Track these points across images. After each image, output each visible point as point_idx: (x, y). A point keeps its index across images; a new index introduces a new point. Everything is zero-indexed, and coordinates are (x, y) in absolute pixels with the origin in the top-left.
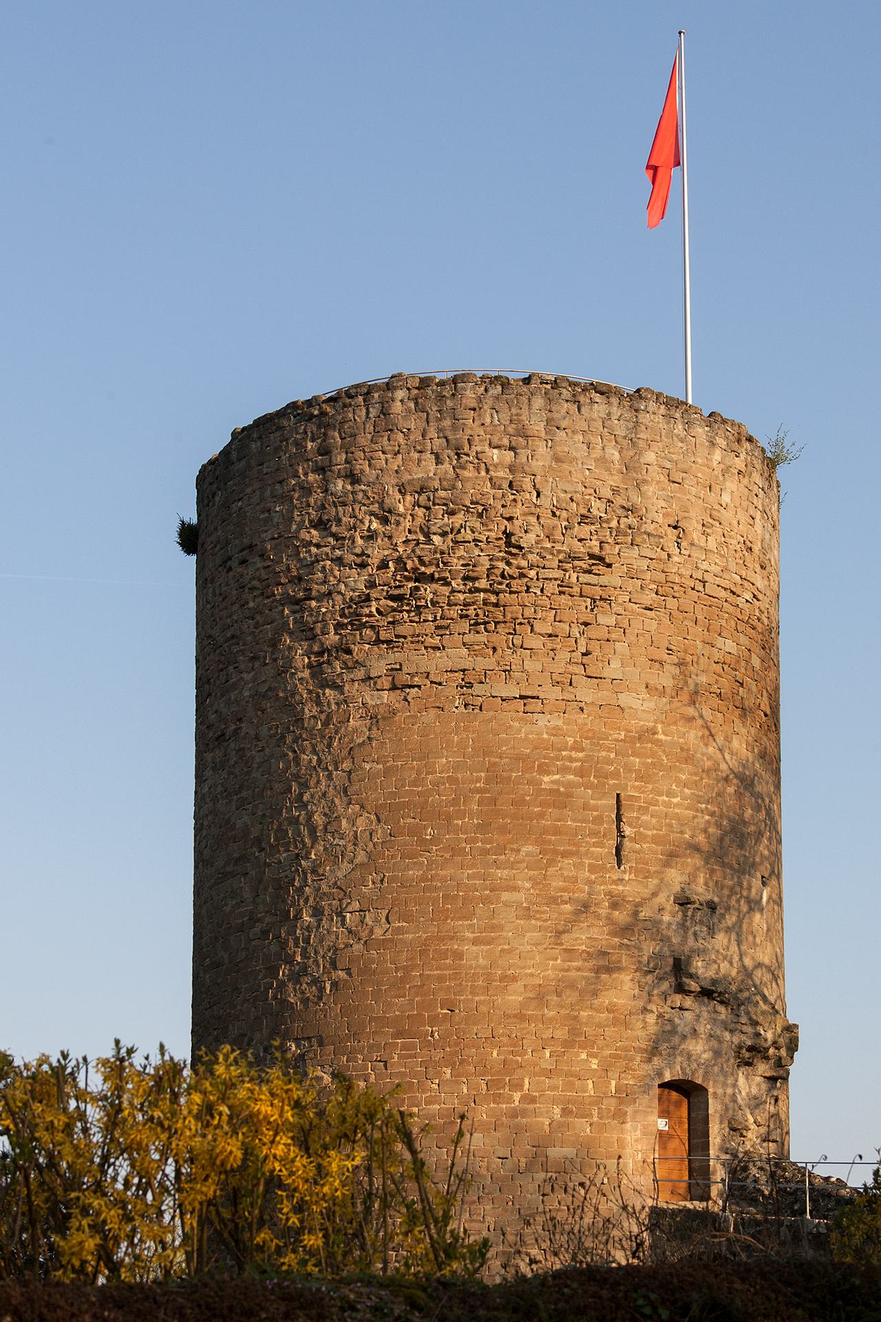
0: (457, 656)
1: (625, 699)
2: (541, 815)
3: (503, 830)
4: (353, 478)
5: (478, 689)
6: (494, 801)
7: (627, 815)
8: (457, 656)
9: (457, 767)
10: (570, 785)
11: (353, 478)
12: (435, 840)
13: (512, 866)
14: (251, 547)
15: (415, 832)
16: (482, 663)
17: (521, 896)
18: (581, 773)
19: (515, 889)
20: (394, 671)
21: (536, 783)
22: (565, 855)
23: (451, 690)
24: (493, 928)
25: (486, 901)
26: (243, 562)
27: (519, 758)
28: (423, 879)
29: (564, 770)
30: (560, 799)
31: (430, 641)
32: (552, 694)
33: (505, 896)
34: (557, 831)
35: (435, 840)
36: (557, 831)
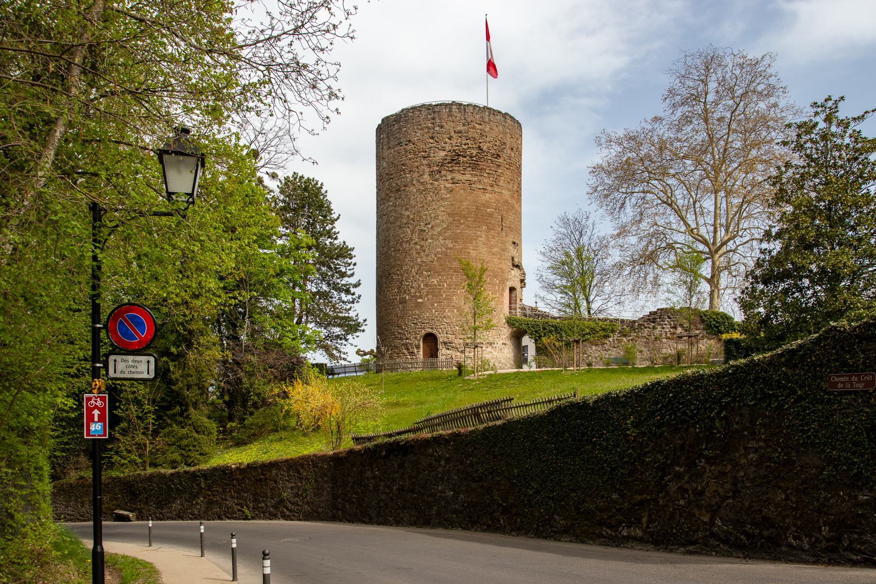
0: (468, 177)
1: (503, 191)
2: (487, 219)
3: (479, 222)
4: (442, 127)
5: (473, 186)
6: (477, 215)
7: (504, 221)
8: (468, 177)
9: (468, 205)
10: (493, 212)
11: (442, 127)
12: (464, 223)
13: (481, 231)
14: (409, 141)
15: (459, 221)
16: (474, 179)
17: (483, 239)
18: (495, 209)
19: (482, 237)
20: (452, 179)
21: (486, 211)
22: (492, 229)
23: (467, 185)
24: (477, 247)
25: (475, 239)
26: (406, 145)
27: (483, 204)
28: (460, 233)
29: (492, 208)
30: (491, 215)
31: (462, 172)
32: (489, 188)
33: (480, 239)
34: (490, 223)
35: (464, 223)
36: (490, 223)
